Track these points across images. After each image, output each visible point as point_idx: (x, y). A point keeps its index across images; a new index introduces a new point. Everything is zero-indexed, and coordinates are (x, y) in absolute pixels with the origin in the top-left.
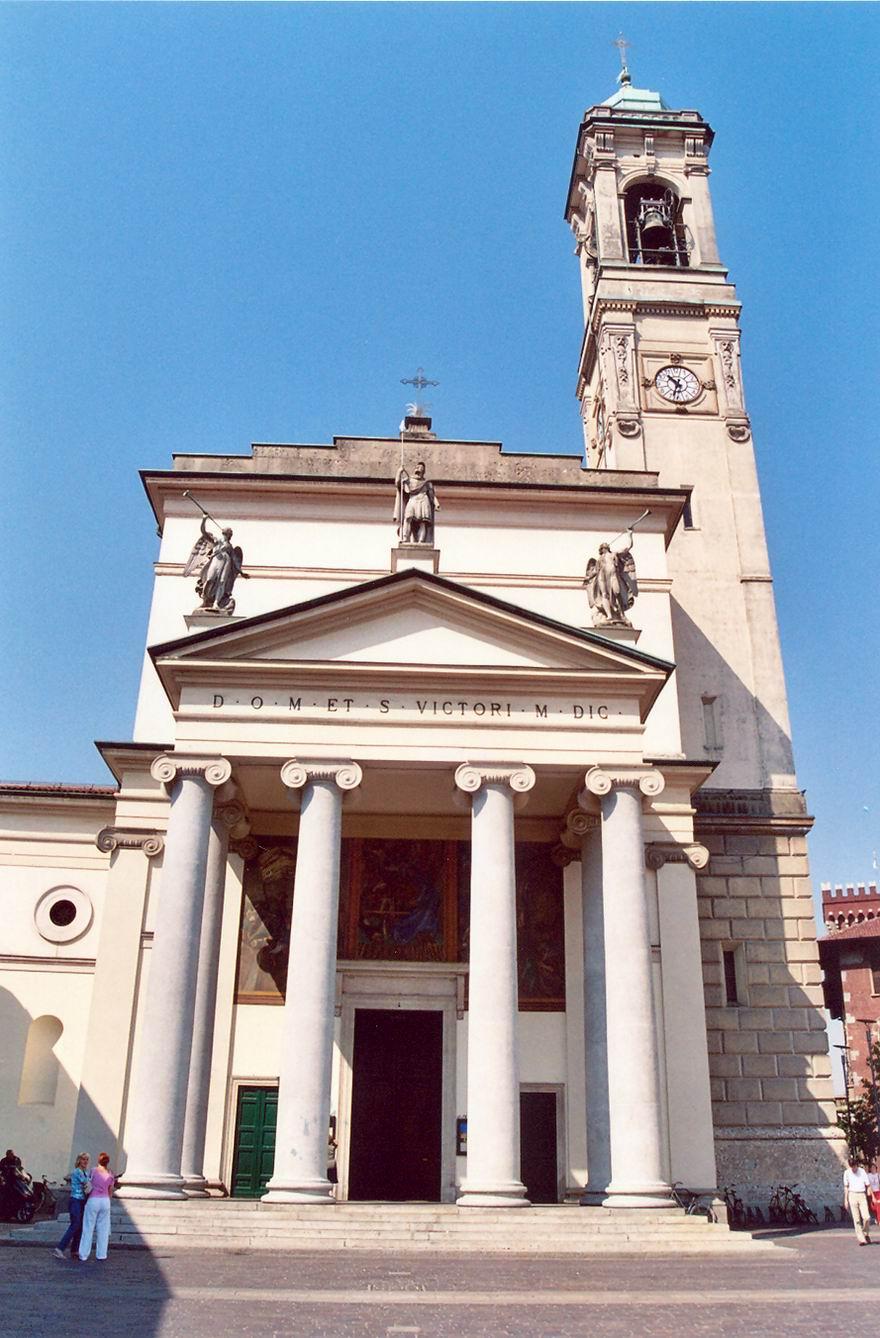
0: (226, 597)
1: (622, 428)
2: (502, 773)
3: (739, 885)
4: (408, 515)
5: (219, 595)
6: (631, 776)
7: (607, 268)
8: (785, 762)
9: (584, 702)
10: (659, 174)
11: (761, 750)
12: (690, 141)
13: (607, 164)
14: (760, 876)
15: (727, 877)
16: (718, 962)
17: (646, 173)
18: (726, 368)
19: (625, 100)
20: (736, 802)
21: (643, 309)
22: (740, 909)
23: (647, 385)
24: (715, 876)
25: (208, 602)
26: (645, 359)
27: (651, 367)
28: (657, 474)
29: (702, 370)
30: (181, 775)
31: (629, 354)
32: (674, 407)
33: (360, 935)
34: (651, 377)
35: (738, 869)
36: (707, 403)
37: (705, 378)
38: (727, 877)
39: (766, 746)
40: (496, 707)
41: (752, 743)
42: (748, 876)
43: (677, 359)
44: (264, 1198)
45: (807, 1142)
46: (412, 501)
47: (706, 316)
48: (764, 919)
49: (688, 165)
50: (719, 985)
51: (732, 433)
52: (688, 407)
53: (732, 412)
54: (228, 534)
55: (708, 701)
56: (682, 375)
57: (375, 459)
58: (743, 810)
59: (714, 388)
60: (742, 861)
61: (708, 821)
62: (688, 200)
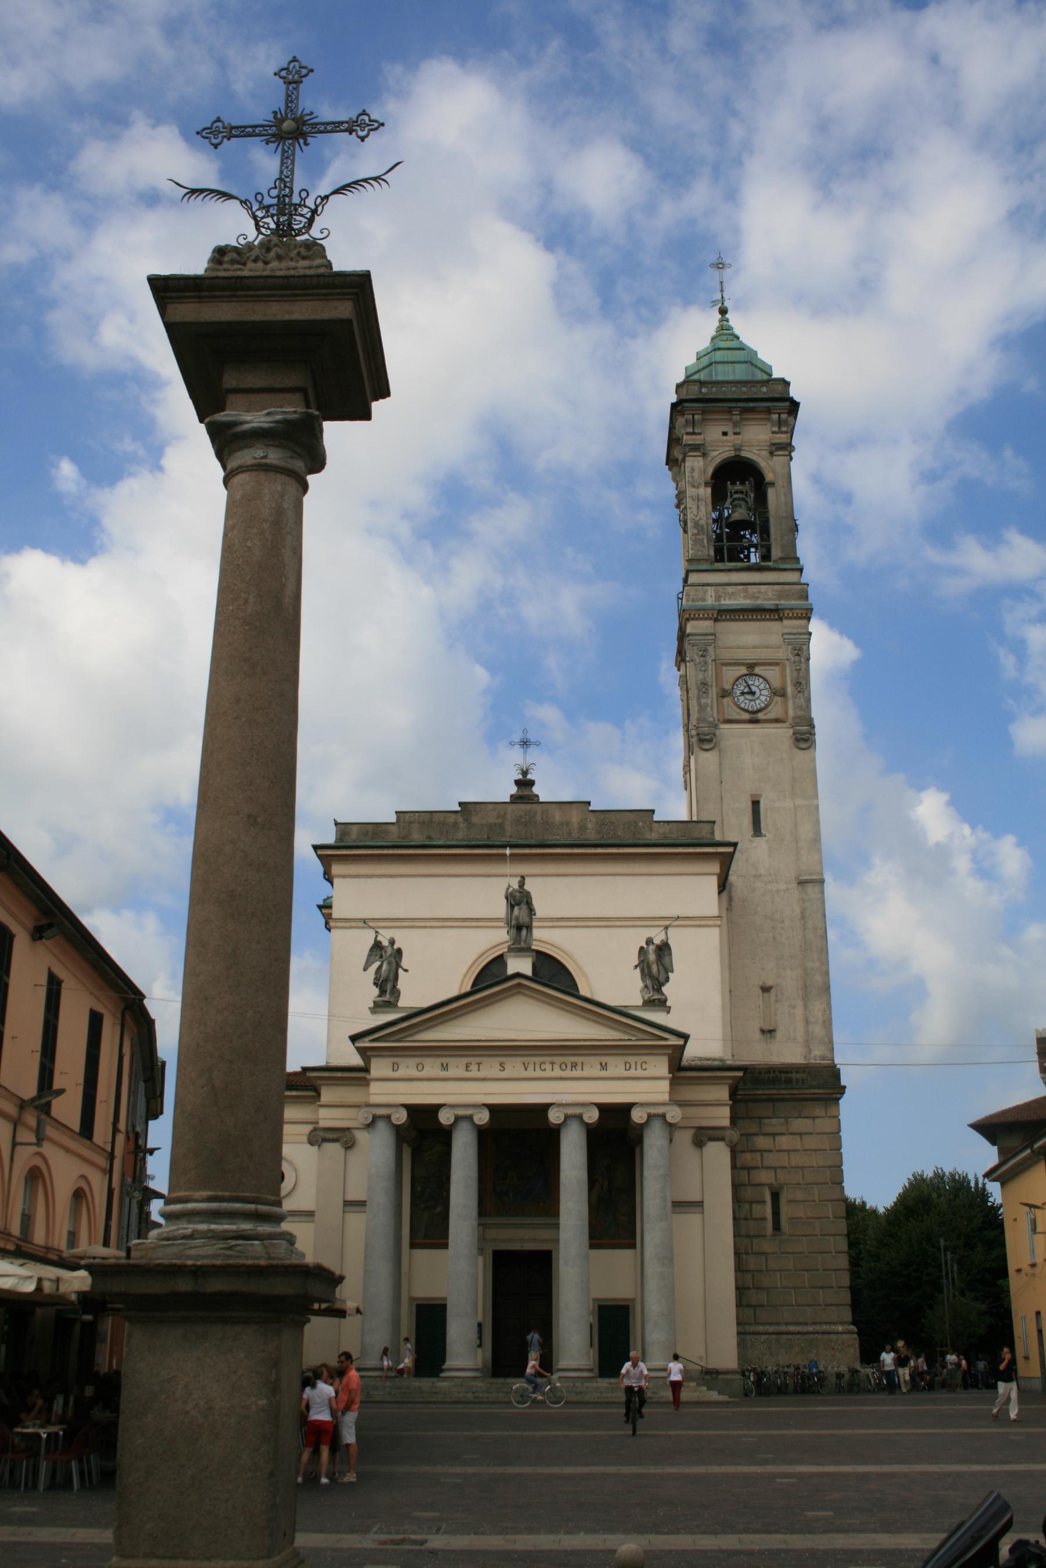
0: (396, 993)
1: (701, 741)
2: (577, 1111)
3: (784, 1142)
4: (514, 923)
5: (389, 987)
6: (660, 1110)
7: (692, 571)
8: (826, 1040)
9: (632, 1060)
10: (744, 454)
11: (807, 1032)
12: (775, 417)
13: (695, 448)
14: (801, 1134)
15: (774, 1135)
16: (764, 1202)
17: (732, 454)
18: (795, 674)
19: (716, 363)
20: (783, 1076)
21: (723, 614)
22: (783, 1160)
23: (724, 694)
24: (765, 1134)
25: (383, 992)
26: (724, 668)
27: (731, 674)
28: (714, 822)
29: (772, 674)
30: (375, 1118)
31: (711, 667)
32: (746, 716)
33: (492, 1201)
34: (727, 687)
35: (783, 1129)
36: (774, 712)
37: (776, 684)
38: (774, 1135)
39: (811, 1028)
40: (574, 1066)
41: (800, 1025)
42: (791, 1134)
43: (751, 666)
44: (442, 1375)
45: (826, 1336)
46: (516, 909)
47: (781, 619)
48: (802, 1168)
49: (773, 444)
50: (764, 1219)
51: (798, 740)
52: (760, 716)
53: (798, 720)
54: (392, 942)
55: (766, 989)
56: (757, 683)
57: (492, 820)
58: (789, 1081)
59: (783, 695)
60: (787, 1122)
61: (760, 1092)
62: (772, 484)
